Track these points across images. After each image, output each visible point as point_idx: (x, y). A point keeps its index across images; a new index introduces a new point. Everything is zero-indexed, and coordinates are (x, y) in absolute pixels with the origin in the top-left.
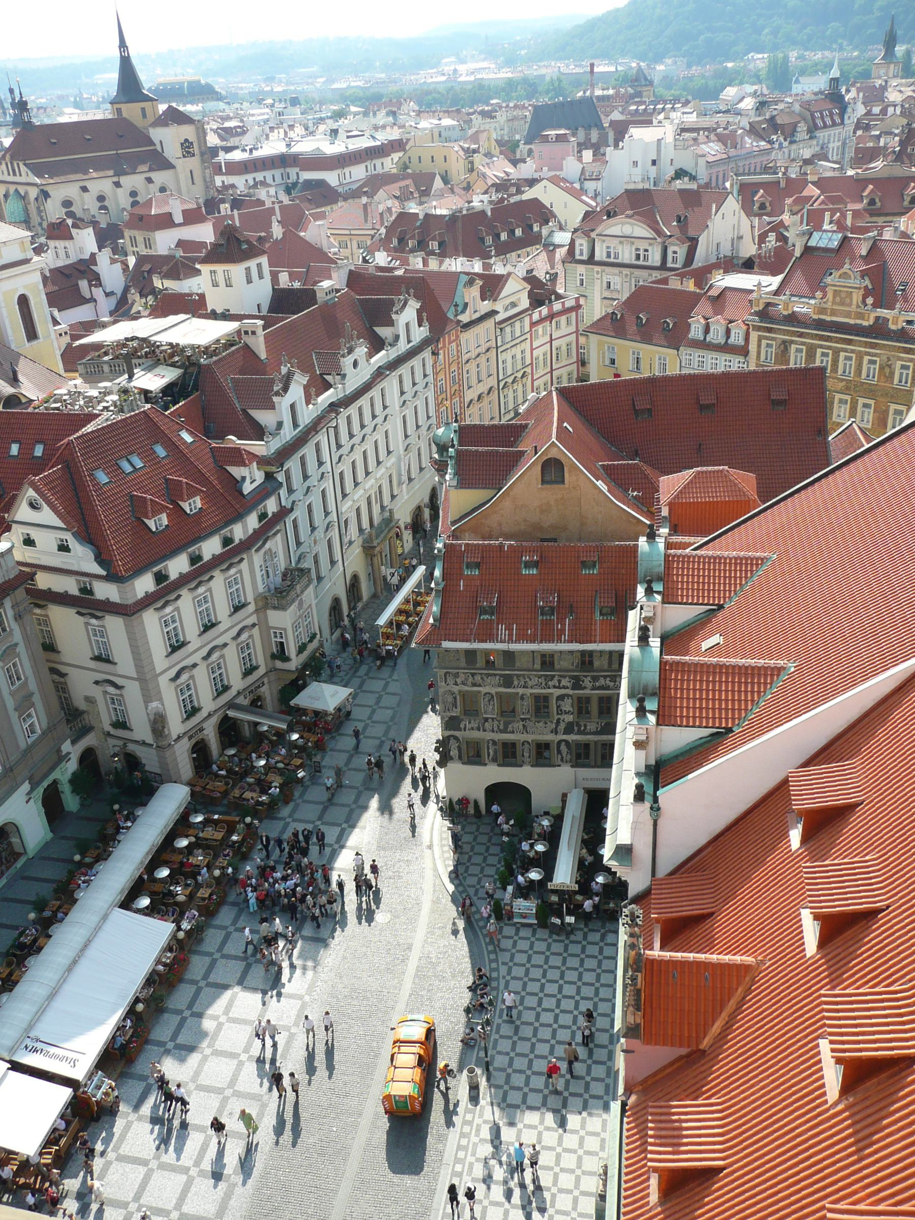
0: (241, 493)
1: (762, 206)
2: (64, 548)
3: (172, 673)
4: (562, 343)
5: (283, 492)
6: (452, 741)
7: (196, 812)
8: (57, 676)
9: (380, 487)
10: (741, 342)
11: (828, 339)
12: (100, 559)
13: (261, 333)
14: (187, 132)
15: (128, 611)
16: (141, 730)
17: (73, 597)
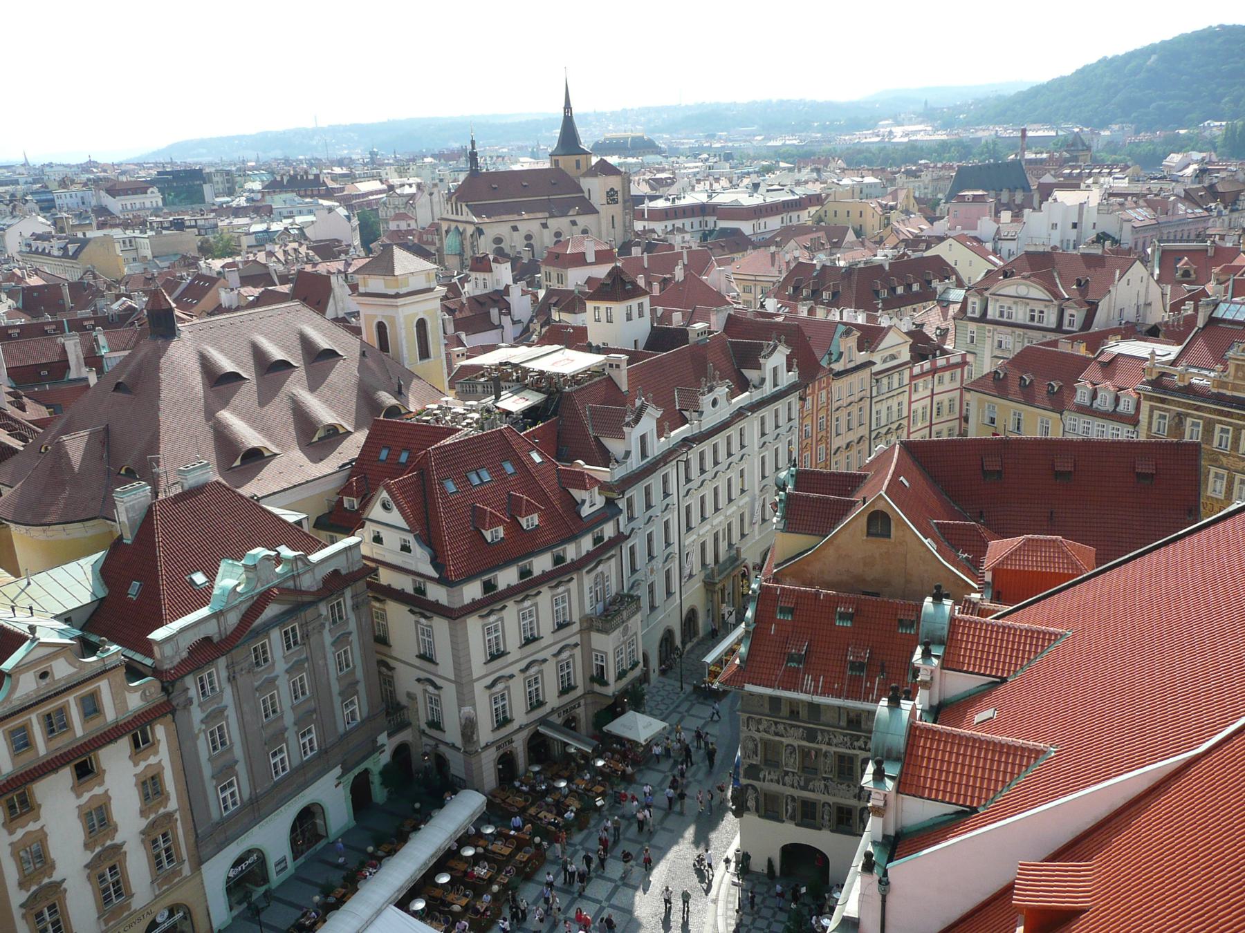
0: (579, 515)
1: (1186, 274)
2: (405, 548)
3: (489, 680)
4: (945, 398)
5: (623, 519)
6: (750, 791)
7: (489, 823)
8: (384, 669)
9: (729, 525)
10: (1131, 411)
11: (1228, 415)
12: (435, 562)
13: (624, 366)
14: (614, 182)
15: (454, 614)
16: (452, 733)
17: (409, 595)
